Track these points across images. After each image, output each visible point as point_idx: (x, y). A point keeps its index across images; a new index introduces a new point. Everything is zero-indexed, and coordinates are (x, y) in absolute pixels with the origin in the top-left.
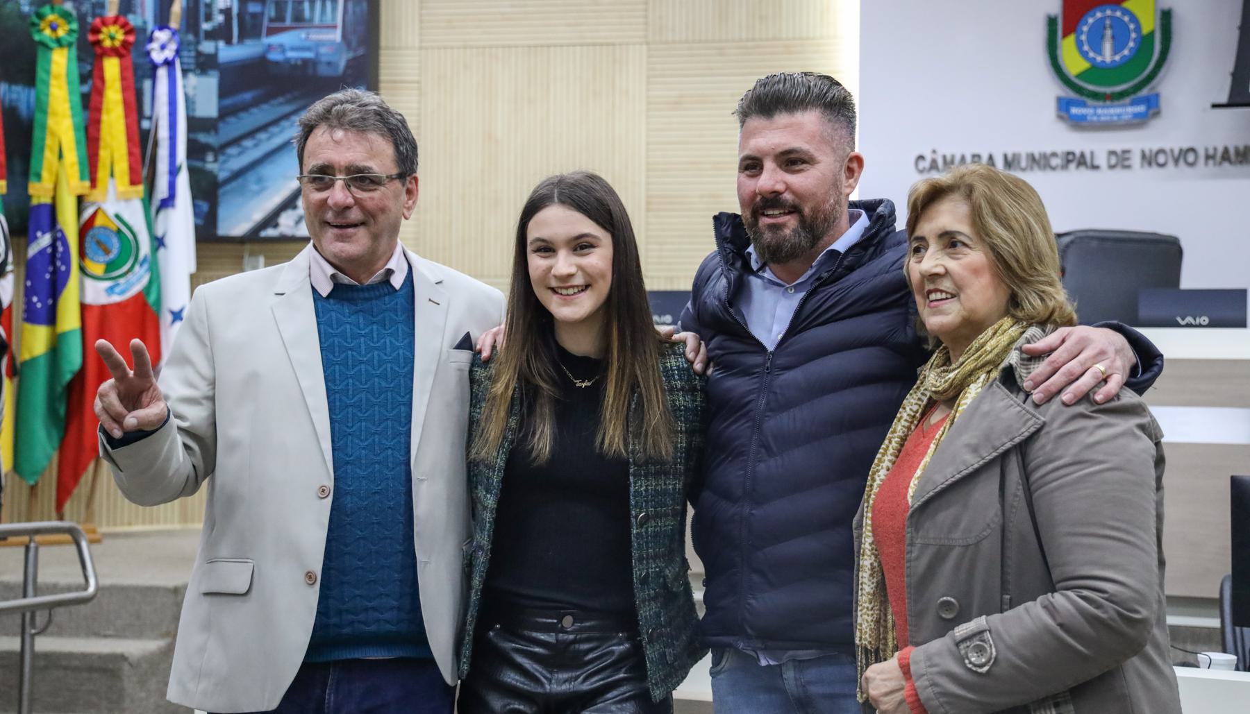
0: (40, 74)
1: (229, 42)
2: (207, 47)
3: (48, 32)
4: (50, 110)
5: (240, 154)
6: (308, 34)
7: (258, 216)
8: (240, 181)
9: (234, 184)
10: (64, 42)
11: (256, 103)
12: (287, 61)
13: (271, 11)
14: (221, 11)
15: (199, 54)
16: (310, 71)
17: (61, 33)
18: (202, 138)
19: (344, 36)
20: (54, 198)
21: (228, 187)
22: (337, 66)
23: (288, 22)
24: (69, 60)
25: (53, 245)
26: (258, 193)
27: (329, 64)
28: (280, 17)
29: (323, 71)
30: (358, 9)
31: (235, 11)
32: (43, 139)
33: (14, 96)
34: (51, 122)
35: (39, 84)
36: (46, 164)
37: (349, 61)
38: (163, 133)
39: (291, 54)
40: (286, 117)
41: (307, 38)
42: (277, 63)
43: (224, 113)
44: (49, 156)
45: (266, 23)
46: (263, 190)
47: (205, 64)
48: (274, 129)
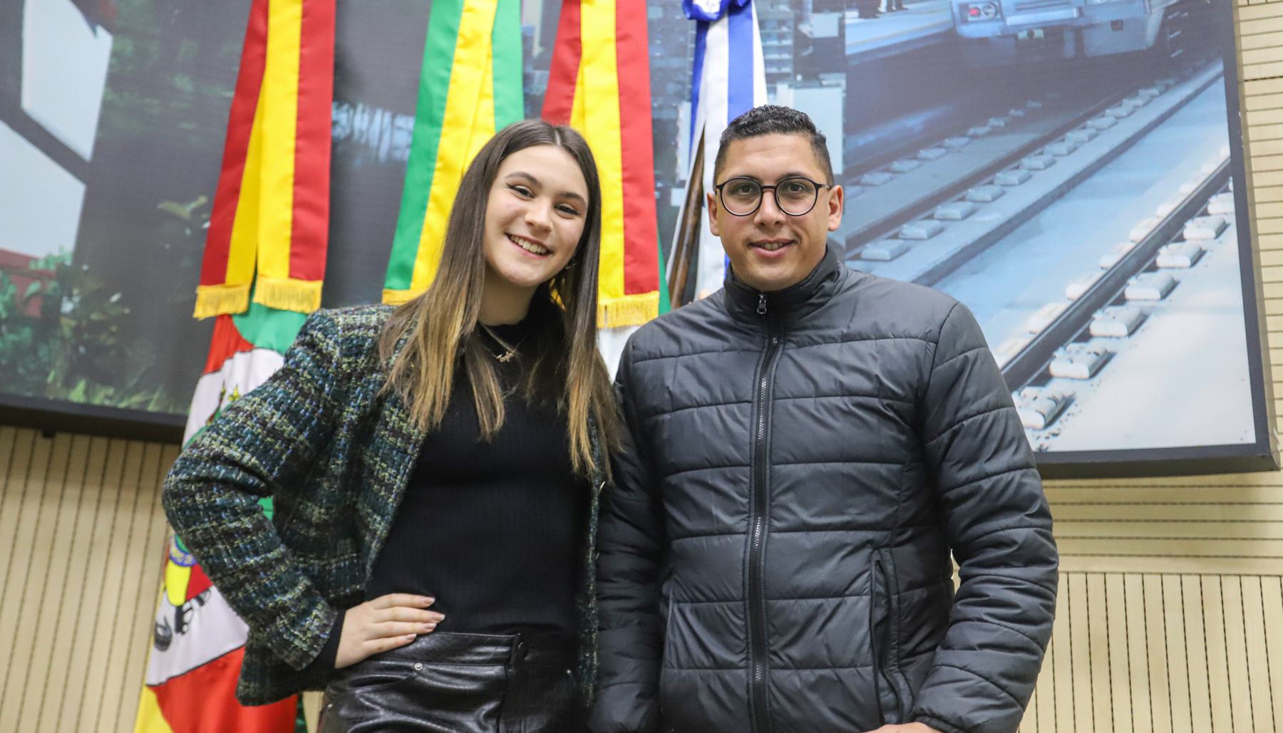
0: (435, 37)
2: (821, 25)
4: (448, 116)
11: (933, 137)
12: (1009, 35)
15: (802, 40)
16: (1069, 49)
22: (1142, 24)
27: (1117, 25)
29: (1101, 44)
32: (428, 184)
33: (402, 138)
37: (1168, 10)
39: (1012, 20)
40: (1010, 160)
42: (983, 42)
43: (858, 165)
48: (980, 193)
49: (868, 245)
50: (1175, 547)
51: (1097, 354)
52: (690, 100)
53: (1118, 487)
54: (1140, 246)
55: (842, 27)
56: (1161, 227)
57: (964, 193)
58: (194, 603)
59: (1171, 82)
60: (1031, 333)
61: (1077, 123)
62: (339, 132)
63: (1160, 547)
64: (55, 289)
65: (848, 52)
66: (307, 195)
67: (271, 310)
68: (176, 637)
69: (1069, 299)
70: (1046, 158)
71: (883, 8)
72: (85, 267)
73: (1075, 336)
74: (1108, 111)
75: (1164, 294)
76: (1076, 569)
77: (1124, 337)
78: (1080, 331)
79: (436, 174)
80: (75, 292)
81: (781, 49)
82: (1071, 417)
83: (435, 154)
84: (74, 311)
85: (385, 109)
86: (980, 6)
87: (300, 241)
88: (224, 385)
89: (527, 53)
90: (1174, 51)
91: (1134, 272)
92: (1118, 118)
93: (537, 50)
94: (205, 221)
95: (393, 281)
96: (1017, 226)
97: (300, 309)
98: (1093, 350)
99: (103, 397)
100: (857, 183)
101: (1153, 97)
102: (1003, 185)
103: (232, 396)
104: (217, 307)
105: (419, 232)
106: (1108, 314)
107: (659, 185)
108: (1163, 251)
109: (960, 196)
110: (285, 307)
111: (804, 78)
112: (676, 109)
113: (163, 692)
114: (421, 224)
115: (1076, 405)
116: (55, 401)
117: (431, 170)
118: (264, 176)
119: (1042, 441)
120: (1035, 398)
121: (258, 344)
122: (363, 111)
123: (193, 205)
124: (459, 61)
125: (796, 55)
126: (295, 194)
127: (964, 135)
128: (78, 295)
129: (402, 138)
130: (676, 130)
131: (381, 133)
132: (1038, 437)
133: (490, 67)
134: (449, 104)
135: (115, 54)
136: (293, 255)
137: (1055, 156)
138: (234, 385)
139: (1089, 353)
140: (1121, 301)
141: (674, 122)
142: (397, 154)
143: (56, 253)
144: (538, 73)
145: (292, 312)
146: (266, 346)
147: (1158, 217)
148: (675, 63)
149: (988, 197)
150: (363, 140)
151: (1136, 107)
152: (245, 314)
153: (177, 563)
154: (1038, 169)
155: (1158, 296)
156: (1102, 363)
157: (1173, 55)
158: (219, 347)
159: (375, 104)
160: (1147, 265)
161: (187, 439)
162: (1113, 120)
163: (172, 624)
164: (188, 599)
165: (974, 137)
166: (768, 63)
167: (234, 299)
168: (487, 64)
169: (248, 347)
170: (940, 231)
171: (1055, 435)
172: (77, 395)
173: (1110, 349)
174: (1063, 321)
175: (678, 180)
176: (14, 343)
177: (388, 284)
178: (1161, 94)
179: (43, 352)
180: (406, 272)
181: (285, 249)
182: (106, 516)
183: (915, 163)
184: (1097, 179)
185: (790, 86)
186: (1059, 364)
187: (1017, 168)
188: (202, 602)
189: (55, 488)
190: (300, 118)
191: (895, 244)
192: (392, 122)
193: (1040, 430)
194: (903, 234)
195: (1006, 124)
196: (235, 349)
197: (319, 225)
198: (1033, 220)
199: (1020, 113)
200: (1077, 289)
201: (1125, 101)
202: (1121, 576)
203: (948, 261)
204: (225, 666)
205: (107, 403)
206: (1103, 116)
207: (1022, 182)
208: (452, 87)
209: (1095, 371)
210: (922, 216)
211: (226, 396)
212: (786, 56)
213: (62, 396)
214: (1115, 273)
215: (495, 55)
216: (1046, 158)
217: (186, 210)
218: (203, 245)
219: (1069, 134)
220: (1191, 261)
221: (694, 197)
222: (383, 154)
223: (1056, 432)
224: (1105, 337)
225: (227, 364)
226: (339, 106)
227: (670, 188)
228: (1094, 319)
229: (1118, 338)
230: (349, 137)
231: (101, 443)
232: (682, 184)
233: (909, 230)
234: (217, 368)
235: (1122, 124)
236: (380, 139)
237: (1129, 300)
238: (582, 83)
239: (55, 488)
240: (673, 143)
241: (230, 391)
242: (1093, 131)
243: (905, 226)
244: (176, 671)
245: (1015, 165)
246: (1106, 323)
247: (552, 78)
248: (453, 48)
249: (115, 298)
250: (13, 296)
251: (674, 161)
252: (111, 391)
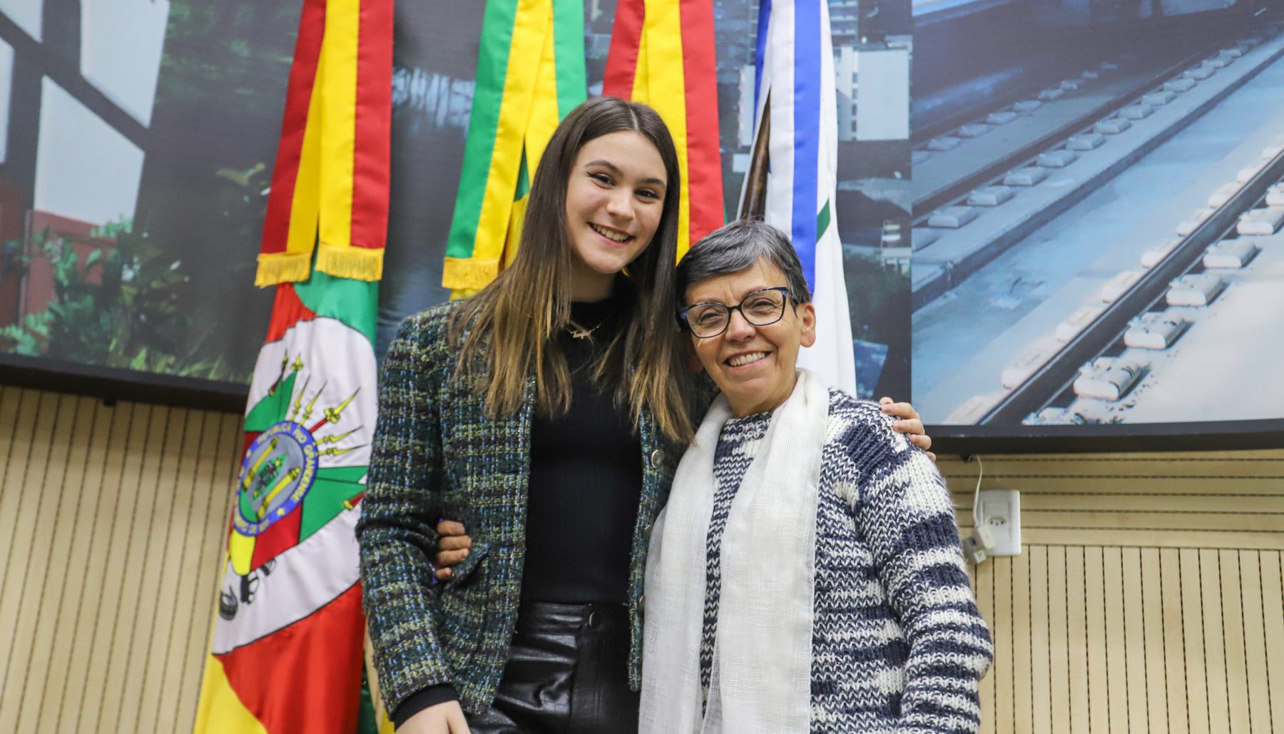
4: (509, 81)
5: (965, 223)
7: (1015, 375)
8: (965, 287)
9: (951, 295)
11: (1002, 100)
18: (873, 189)
21: (939, 302)
26: (1014, 316)
32: (489, 149)
33: (459, 104)
38: (783, 136)
40: (1084, 124)
46: (1020, 312)
48: (1053, 157)
49: (935, 212)
50: (1253, 522)
51: (1174, 324)
52: (752, 64)
53: (1192, 460)
54: (1221, 211)
56: (1242, 192)
57: (1035, 158)
58: (260, 572)
59: (1254, 41)
60: (1105, 302)
61: (1155, 85)
62: (397, 97)
63: (1236, 522)
64: (115, 257)
65: (915, 13)
66: (368, 161)
67: (333, 278)
68: (242, 606)
69: (1145, 267)
70: (1121, 122)
72: (145, 235)
73: (1151, 305)
74: (1187, 73)
75: (1245, 261)
76: (1149, 544)
77: (1203, 306)
78: (1156, 301)
79: (498, 140)
80: (136, 260)
81: (846, 11)
82: (1146, 388)
83: (497, 119)
84: (134, 279)
85: (442, 73)
87: (361, 207)
88: (286, 353)
89: (587, 15)
90: (1258, 10)
91: (1213, 239)
92: (1198, 79)
93: (596, 13)
94: (265, 187)
95: (455, 249)
96: (1090, 192)
97: (361, 277)
98: (1169, 320)
99: (163, 366)
100: (924, 149)
101: (1235, 57)
102: (1076, 150)
103: (294, 365)
104: (279, 275)
105: (481, 199)
106: (1186, 282)
107: (721, 150)
108: (1244, 217)
109: (1031, 161)
110: (346, 275)
111: (869, 41)
112: (738, 72)
113: (229, 661)
114: (484, 191)
115: (1152, 376)
116: (118, 370)
117: (493, 136)
118: (324, 142)
119: (1116, 413)
120: (1109, 369)
121: (320, 312)
122: (420, 76)
123: (251, 172)
124: (519, 25)
125: (861, 17)
126: (356, 161)
127: (1035, 99)
128: (138, 262)
129: (459, 104)
130: (738, 93)
131: (439, 99)
132: (1112, 409)
133: (551, 29)
134: (510, 68)
135: (172, 19)
136: (354, 222)
137: (1131, 119)
138: (297, 354)
139: (1166, 323)
140: (1200, 269)
141: (736, 85)
142: (455, 120)
143: (116, 220)
144: (597, 37)
145: (354, 280)
146: (328, 314)
147: (1239, 182)
148: (737, 25)
149: (1060, 163)
150: (420, 106)
151: (1217, 68)
152: (307, 282)
153: (240, 531)
154: (1113, 134)
155: (1239, 264)
156: (1179, 332)
157: (1257, 14)
158: (280, 314)
159: (431, 70)
160: (1227, 231)
161: (249, 408)
162: (1192, 81)
163: (238, 593)
164: (253, 569)
165: (1046, 100)
166: (834, 25)
167: (296, 267)
168: (549, 27)
169: (311, 316)
170: (1011, 197)
171: (1130, 407)
172: (139, 363)
173: (1187, 319)
174: (1140, 289)
175: (739, 146)
176: (77, 311)
177: (449, 252)
178: (1243, 54)
179: (105, 320)
180: (468, 241)
181: (347, 217)
182: (167, 484)
183: (984, 127)
184: (1175, 142)
185: (855, 49)
186: (1134, 334)
187: (1091, 132)
188: (267, 572)
189: (116, 456)
190: (361, 81)
191: (963, 211)
192: (450, 88)
193: (1114, 401)
194: (972, 201)
195: (1079, 87)
196: (297, 318)
197: (379, 192)
198: (1107, 186)
199: (1094, 75)
200: (1153, 257)
201: (1205, 62)
202: (1197, 551)
203: (1018, 227)
204: (291, 636)
205: (168, 371)
206: (1182, 78)
207: (1096, 146)
208: (513, 51)
209: (1172, 341)
210: (991, 182)
211: (289, 365)
212: (850, 18)
213: (123, 366)
214: (1192, 241)
215: (556, 18)
216: (1121, 122)
217: (244, 177)
218: (264, 212)
219: (1145, 97)
220: (1274, 227)
221: (759, 163)
222: (440, 120)
223: (1131, 403)
224: (1183, 306)
225: (290, 332)
226: (397, 70)
227: (732, 154)
228: (1171, 287)
229: (1197, 307)
230: (407, 102)
231: (160, 412)
232: (746, 150)
233: (978, 196)
234: (279, 337)
235: (1201, 85)
236: (438, 105)
237: (1207, 268)
238: (646, 47)
239: (116, 456)
240: (735, 108)
241: (292, 360)
242: (1171, 93)
243: (973, 192)
244: (243, 641)
245: (1089, 128)
246: (1184, 292)
247: (613, 41)
248: (514, 11)
249: (175, 266)
250: (75, 264)
251: (735, 127)
252: (172, 360)
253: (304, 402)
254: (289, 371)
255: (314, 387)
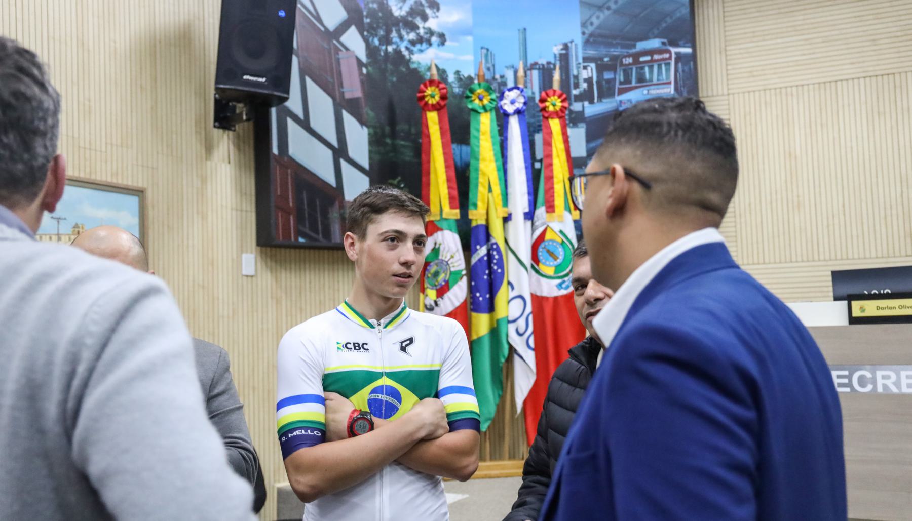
0: (473, 131)
1: (591, 102)
2: (577, 107)
3: (477, 101)
4: (481, 157)
6: (648, 90)
10: (488, 108)
13: (620, 77)
14: (585, 80)
15: (571, 112)
17: (486, 102)
19: (676, 89)
20: (487, 220)
23: (634, 84)
24: (492, 121)
25: (489, 254)
28: (627, 80)
30: (686, 69)
31: (595, 79)
32: (477, 178)
34: (482, 166)
35: (473, 141)
36: (479, 195)
41: (648, 94)
43: (590, 154)
44: (482, 190)
45: (617, 85)
47: (577, 119)
55: (583, 107)
67: (446, 219)
71: (596, 100)
86: (626, 101)
87: (451, 198)
95: (471, 207)
117: (478, 174)
121: (444, 228)
135: (369, 134)
153: (430, 288)
168: (490, 140)
169: (441, 230)
180: (475, 205)
188: (442, 299)
241: (438, 243)
253: (444, 254)
254: (437, 246)
255: (447, 249)
